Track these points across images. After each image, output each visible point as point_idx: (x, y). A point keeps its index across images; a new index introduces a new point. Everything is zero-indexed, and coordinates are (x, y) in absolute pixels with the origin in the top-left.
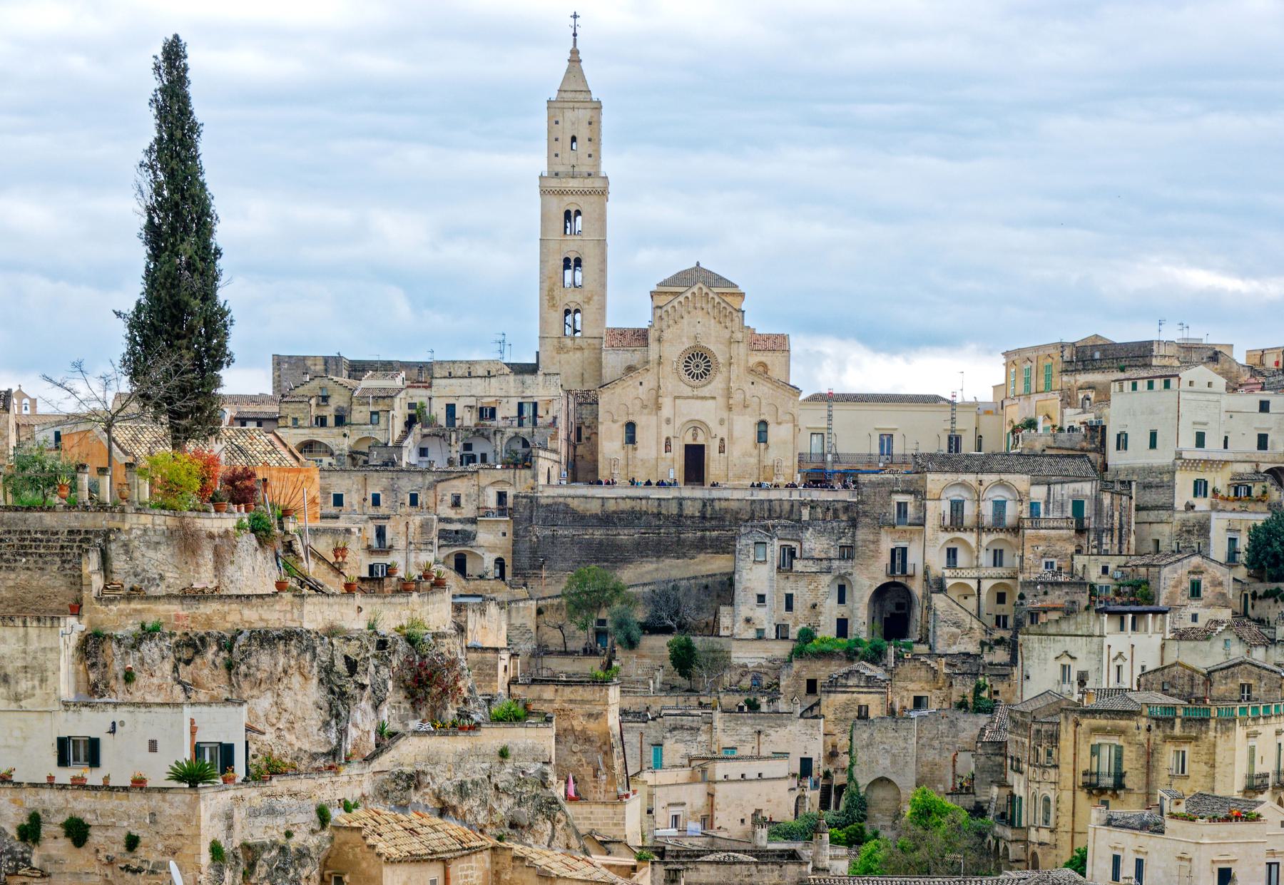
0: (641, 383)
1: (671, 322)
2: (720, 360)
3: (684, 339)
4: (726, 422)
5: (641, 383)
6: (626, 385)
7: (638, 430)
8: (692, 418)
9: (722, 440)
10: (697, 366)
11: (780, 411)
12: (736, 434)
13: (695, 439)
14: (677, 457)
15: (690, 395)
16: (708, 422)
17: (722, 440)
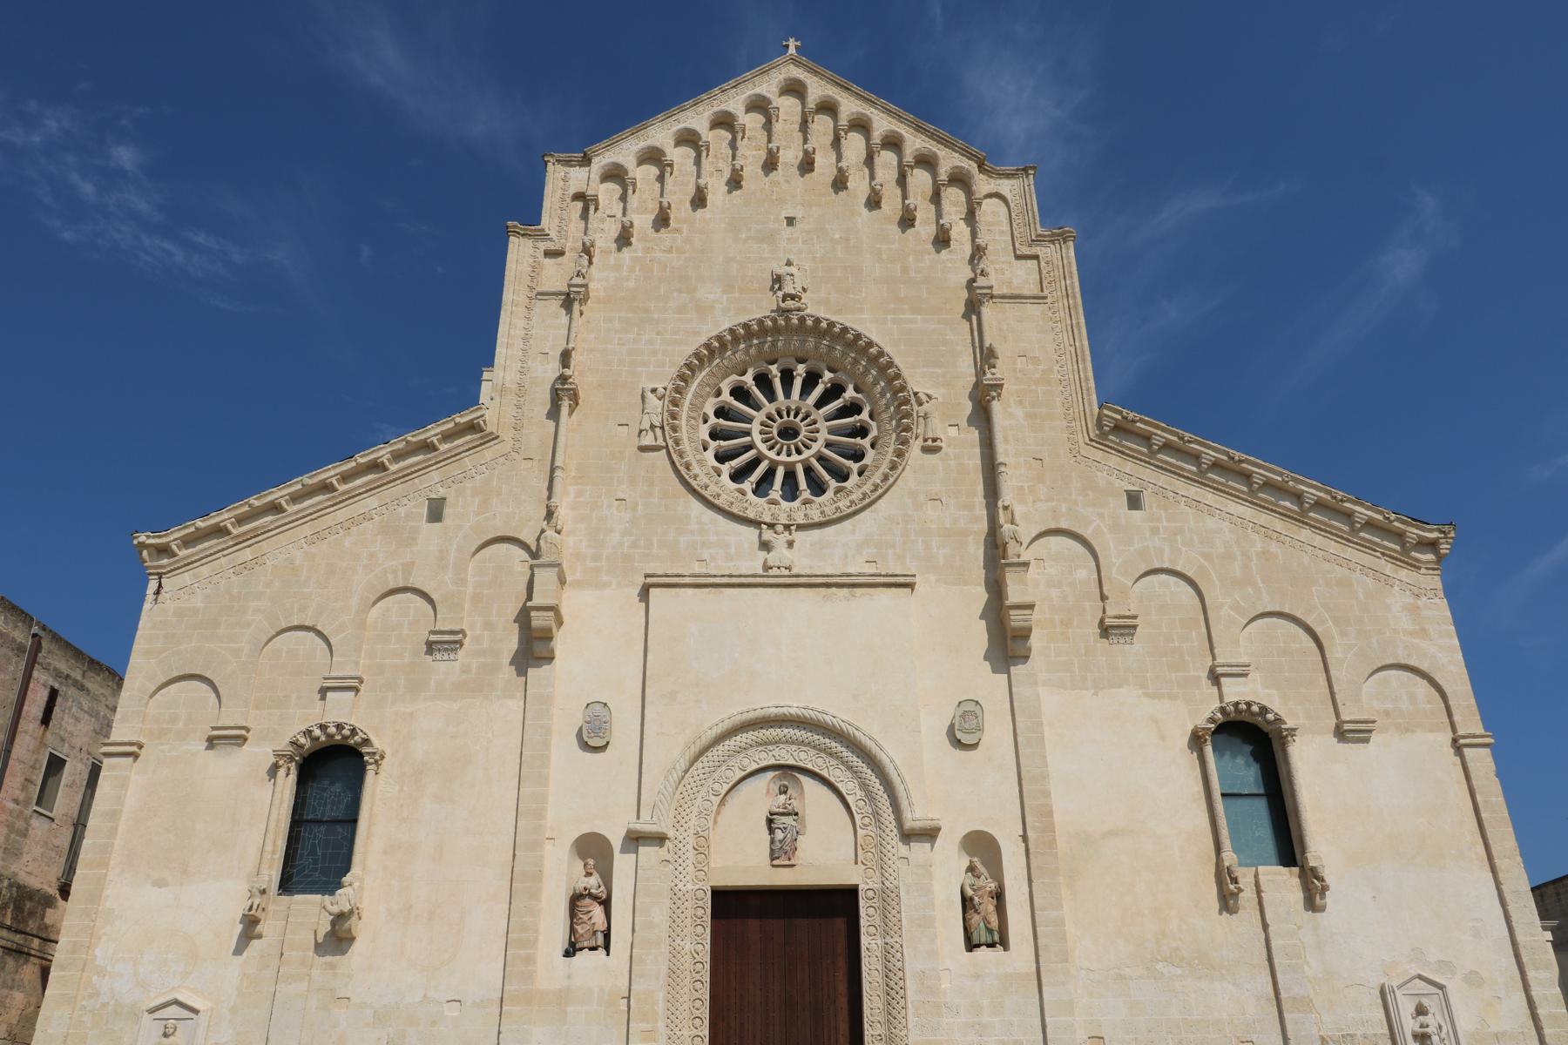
0: (436, 512)
1: (642, 221)
2: (917, 382)
3: (710, 293)
4: (996, 733)
5: (436, 512)
6: (342, 514)
7: (378, 792)
8: (767, 704)
9: (981, 847)
10: (789, 433)
11: (1335, 653)
12: (1069, 809)
13: (781, 853)
14: (652, 986)
15: (752, 564)
16: (869, 729)
17: (981, 847)
